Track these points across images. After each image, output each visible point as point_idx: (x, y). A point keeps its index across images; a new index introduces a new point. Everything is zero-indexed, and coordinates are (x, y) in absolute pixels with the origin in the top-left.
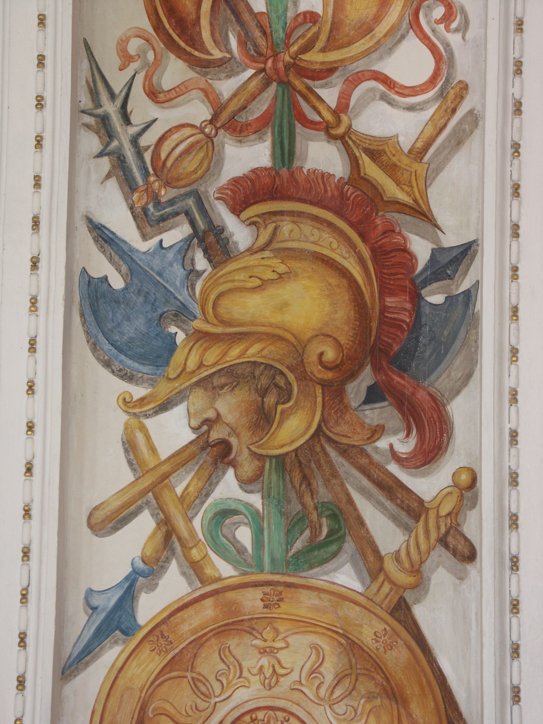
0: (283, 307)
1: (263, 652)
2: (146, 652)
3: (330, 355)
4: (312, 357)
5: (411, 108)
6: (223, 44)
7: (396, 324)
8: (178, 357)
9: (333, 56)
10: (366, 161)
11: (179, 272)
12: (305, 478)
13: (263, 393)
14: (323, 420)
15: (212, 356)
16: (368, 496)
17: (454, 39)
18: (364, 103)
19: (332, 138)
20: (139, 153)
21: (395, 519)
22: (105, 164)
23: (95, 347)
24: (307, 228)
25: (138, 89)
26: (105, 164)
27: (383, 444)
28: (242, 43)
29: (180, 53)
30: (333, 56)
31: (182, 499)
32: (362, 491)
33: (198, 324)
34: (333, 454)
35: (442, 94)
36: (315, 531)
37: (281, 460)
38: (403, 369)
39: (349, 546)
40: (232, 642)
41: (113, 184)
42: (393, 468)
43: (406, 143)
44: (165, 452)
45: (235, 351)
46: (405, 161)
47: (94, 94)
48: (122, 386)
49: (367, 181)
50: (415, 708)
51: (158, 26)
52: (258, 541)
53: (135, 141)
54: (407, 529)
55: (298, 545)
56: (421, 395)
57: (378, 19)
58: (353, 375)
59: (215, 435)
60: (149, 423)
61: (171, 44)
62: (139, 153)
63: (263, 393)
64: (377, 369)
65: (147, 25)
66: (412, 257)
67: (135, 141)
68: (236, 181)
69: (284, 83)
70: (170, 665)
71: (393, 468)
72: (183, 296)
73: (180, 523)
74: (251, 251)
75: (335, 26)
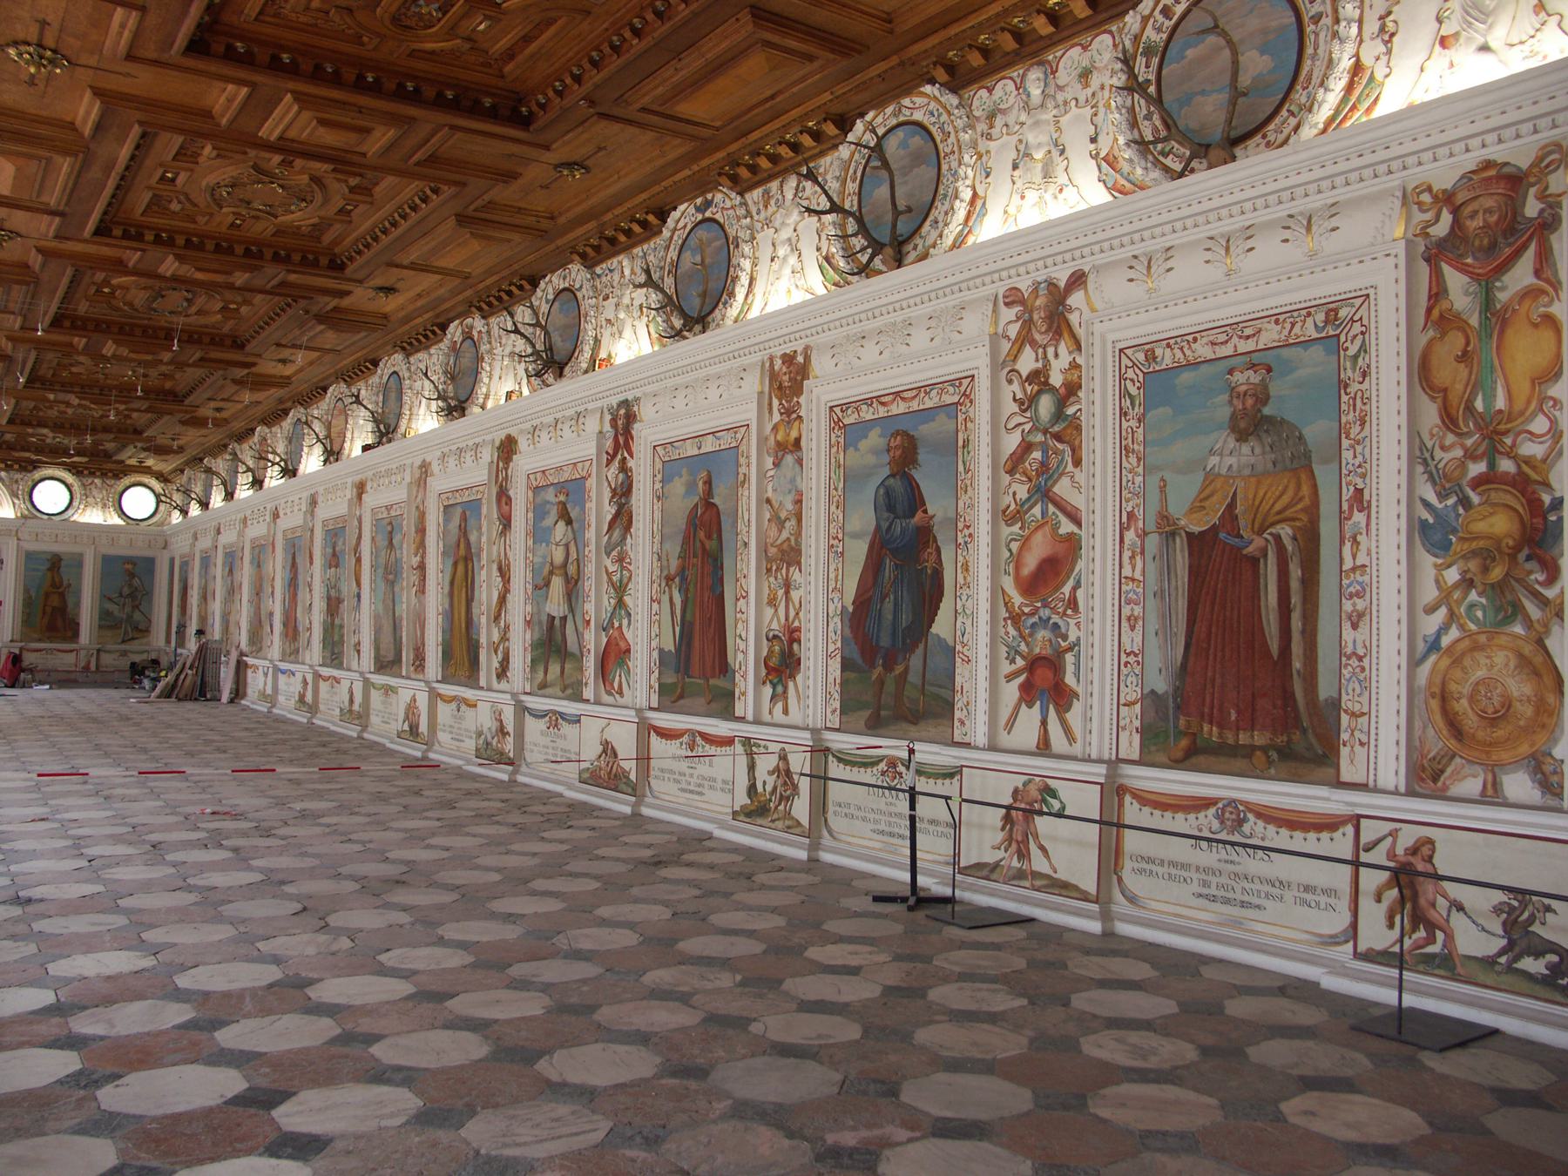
0: (1492, 526)
1: (1488, 657)
2: (1444, 658)
3: (1511, 543)
4: (1504, 545)
5: (1541, 443)
6: (1468, 427)
7: (1536, 529)
8: (1453, 547)
9: (1509, 426)
10: (1523, 465)
11: (1453, 515)
12: (1502, 592)
13: (1485, 559)
14: (1509, 569)
15: (1466, 546)
16: (1527, 598)
17: (1557, 413)
18: (1522, 442)
19: (1510, 458)
20: (1438, 470)
21: (1538, 606)
22: (1426, 476)
23: (1424, 545)
24: (1501, 494)
25: (1437, 447)
26: (1426, 476)
27: (1532, 577)
28: (1475, 425)
29: (1452, 431)
30: (1509, 426)
31: (1456, 601)
32: (1525, 596)
33: (1461, 534)
34: (1513, 582)
35: (1553, 436)
36: (1506, 612)
37: (1493, 586)
38: (1540, 547)
39: (1519, 617)
40: (1475, 654)
41: (1429, 484)
42: (1537, 586)
43: (1539, 457)
44: (1450, 583)
45: (1474, 544)
46: (1538, 464)
47: (1421, 450)
48: (1434, 559)
49: (1524, 473)
50: (1545, 679)
51: (1443, 421)
52: (1484, 616)
53: (1436, 466)
54: (1543, 610)
55: (1500, 617)
56: (1548, 557)
57: (1526, 409)
58: (1520, 551)
59: (1468, 576)
60: (1444, 573)
61: (1448, 428)
62: (1438, 470)
63: (1485, 559)
64: (1530, 548)
65: (1438, 421)
66: (1541, 501)
67: (1436, 466)
68: (1473, 478)
69: (1491, 438)
70: (1453, 662)
71: (1537, 586)
72: (1455, 524)
73: (1456, 611)
74: (1479, 505)
75: (1510, 414)
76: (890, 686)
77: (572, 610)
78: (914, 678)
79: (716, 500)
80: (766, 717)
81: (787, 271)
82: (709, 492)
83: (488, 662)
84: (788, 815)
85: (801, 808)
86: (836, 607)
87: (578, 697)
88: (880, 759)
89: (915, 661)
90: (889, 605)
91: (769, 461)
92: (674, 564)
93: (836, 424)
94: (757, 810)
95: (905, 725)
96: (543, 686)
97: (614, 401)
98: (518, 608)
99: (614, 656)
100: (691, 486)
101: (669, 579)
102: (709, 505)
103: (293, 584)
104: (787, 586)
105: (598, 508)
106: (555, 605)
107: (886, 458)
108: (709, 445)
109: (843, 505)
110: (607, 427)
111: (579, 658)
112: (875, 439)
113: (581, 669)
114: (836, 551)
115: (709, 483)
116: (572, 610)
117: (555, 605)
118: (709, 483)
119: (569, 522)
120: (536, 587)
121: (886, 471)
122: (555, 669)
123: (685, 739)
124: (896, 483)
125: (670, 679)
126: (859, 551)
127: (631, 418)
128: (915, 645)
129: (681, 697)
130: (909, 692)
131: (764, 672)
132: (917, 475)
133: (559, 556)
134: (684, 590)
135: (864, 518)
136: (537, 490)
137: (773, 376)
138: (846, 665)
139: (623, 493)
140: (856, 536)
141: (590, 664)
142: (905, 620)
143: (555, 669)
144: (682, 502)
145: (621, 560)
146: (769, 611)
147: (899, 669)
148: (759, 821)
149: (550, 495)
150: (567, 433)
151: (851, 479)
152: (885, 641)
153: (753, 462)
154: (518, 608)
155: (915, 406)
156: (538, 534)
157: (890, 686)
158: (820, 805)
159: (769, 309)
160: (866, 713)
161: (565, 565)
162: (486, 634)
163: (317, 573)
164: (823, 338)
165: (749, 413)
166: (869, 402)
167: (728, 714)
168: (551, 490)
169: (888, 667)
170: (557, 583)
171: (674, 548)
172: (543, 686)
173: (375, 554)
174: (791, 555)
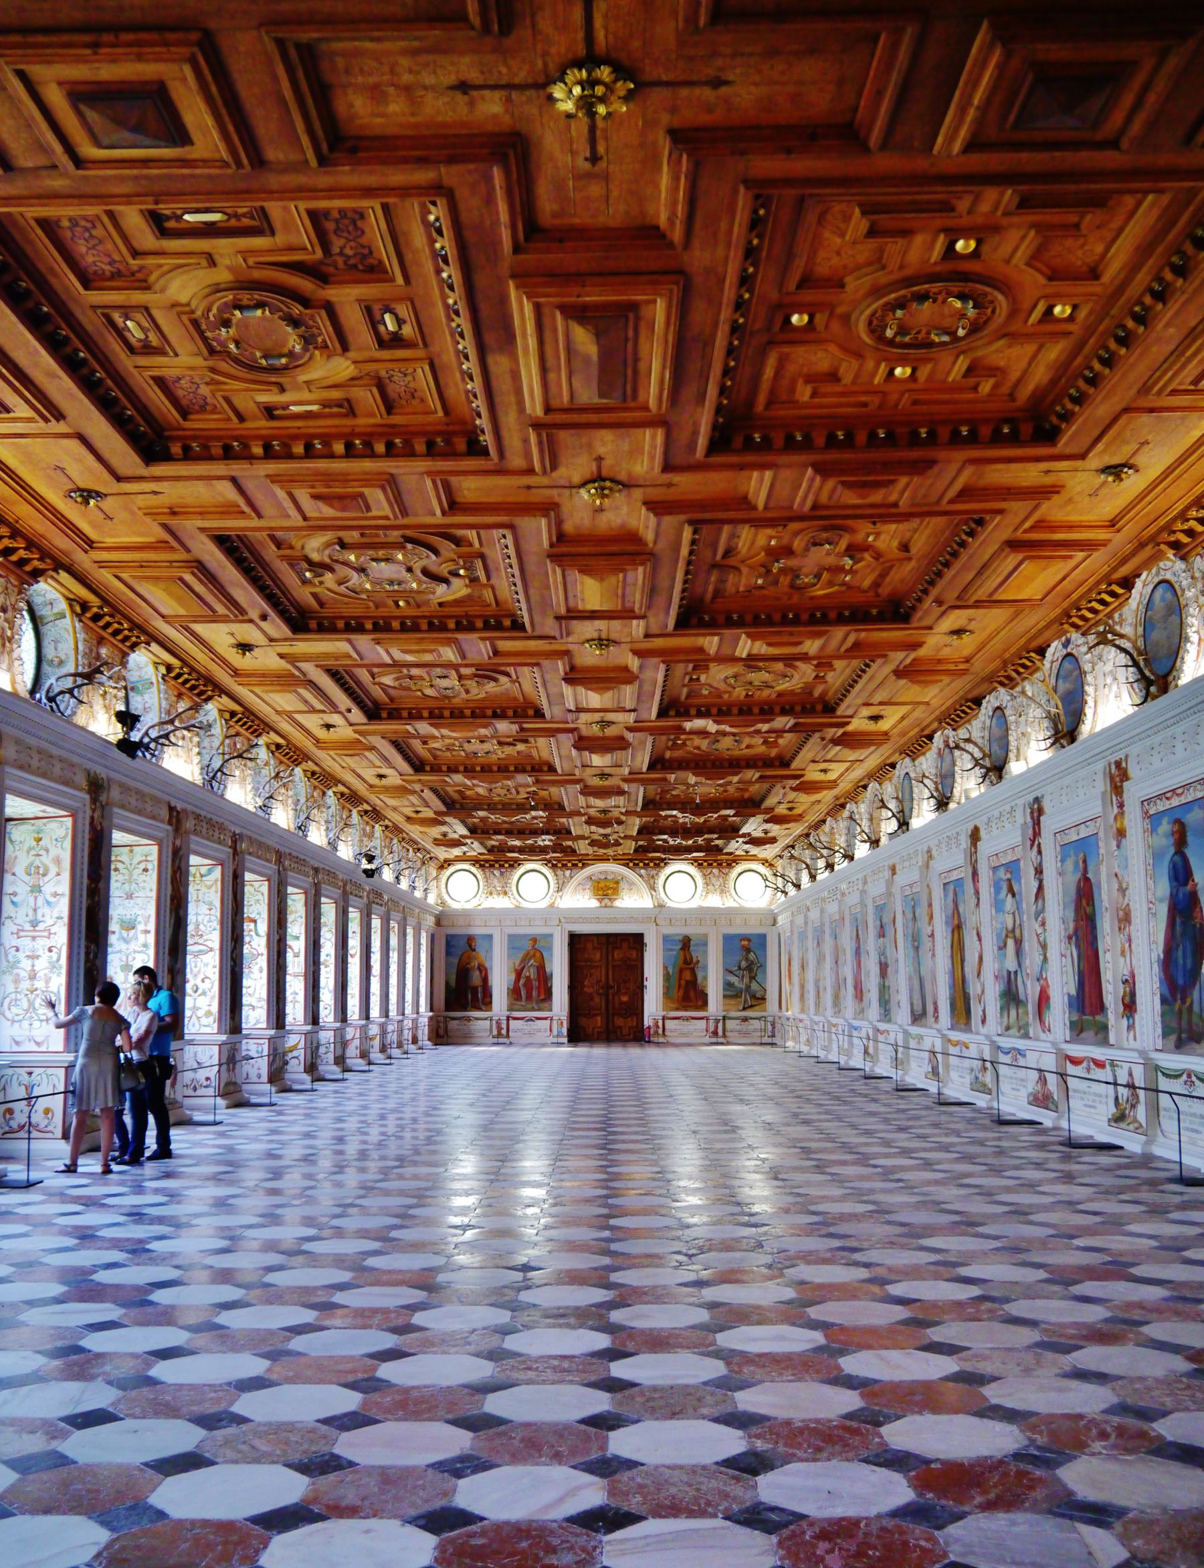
76: (1185, 1016)
77: (1020, 965)
78: (1196, 1008)
79: (1090, 875)
80: (1125, 1045)
81: (1112, 695)
82: (1085, 871)
83: (976, 1011)
84: (1135, 1120)
85: (1141, 1113)
86: (1154, 958)
87: (1026, 1036)
88: (1183, 1071)
89: (1196, 994)
90: (1180, 953)
91: (1114, 843)
92: (1071, 926)
93: (1146, 814)
94: (1119, 1118)
95: (1194, 1045)
96: (1008, 1028)
97: (1031, 798)
98: (990, 967)
99: (1043, 1000)
100: (1076, 864)
101: (1070, 938)
102: (1087, 880)
103: (858, 953)
104: (1130, 941)
105: (1028, 884)
106: (1011, 964)
107: (1171, 840)
108: (1084, 832)
109: (1153, 877)
110: (1029, 819)
111: (1025, 1004)
112: (1165, 827)
113: (1027, 1013)
114: (1152, 914)
115: (1085, 862)
116: (1020, 965)
117: (1011, 964)
118: (1085, 862)
119: (1014, 895)
120: (1000, 948)
121: (1172, 850)
122: (1013, 1013)
123: (1085, 1064)
124: (1177, 858)
125: (1075, 1018)
126: (1163, 910)
127: (1040, 811)
128: (1193, 986)
129: (1081, 1031)
130: (1195, 1019)
131: (1121, 1008)
132: (1189, 852)
133: (1010, 926)
134: (1078, 947)
135: (1164, 887)
136: (995, 869)
137: (1112, 778)
138: (1163, 1001)
139: (1039, 871)
140: (1161, 901)
141: (1031, 1007)
142: (1189, 965)
143: (1013, 1013)
144: (1073, 878)
145: (1043, 924)
146: (1122, 960)
147: (1188, 1001)
148: (1123, 1125)
149: (1002, 874)
150: (1006, 824)
151: (1157, 856)
152: (1181, 981)
153: (1107, 845)
154: (990, 967)
155: (1183, 800)
156: (998, 906)
157: (1185, 1016)
158: (1155, 1110)
159: (1098, 729)
160: (1173, 1038)
161: (1013, 930)
162: (974, 989)
163: (871, 943)
164: (1134, 750)
165: (1097, 810)
166: (1160, 797)
167: (1105, 1042)
168: (1002, 870)
169: (1183, 1001)
170: (1010, 942)
171: (1071, 914)
172: (1008, 1028)
173: (905, 926)
174: (1125, 919)
